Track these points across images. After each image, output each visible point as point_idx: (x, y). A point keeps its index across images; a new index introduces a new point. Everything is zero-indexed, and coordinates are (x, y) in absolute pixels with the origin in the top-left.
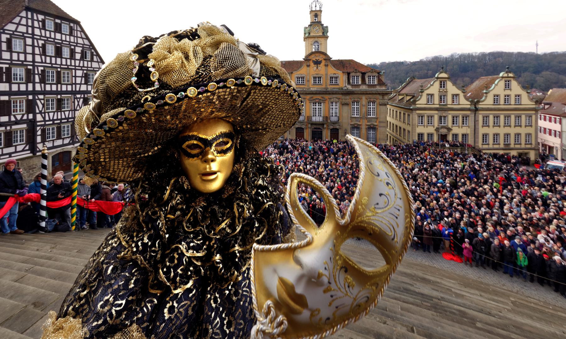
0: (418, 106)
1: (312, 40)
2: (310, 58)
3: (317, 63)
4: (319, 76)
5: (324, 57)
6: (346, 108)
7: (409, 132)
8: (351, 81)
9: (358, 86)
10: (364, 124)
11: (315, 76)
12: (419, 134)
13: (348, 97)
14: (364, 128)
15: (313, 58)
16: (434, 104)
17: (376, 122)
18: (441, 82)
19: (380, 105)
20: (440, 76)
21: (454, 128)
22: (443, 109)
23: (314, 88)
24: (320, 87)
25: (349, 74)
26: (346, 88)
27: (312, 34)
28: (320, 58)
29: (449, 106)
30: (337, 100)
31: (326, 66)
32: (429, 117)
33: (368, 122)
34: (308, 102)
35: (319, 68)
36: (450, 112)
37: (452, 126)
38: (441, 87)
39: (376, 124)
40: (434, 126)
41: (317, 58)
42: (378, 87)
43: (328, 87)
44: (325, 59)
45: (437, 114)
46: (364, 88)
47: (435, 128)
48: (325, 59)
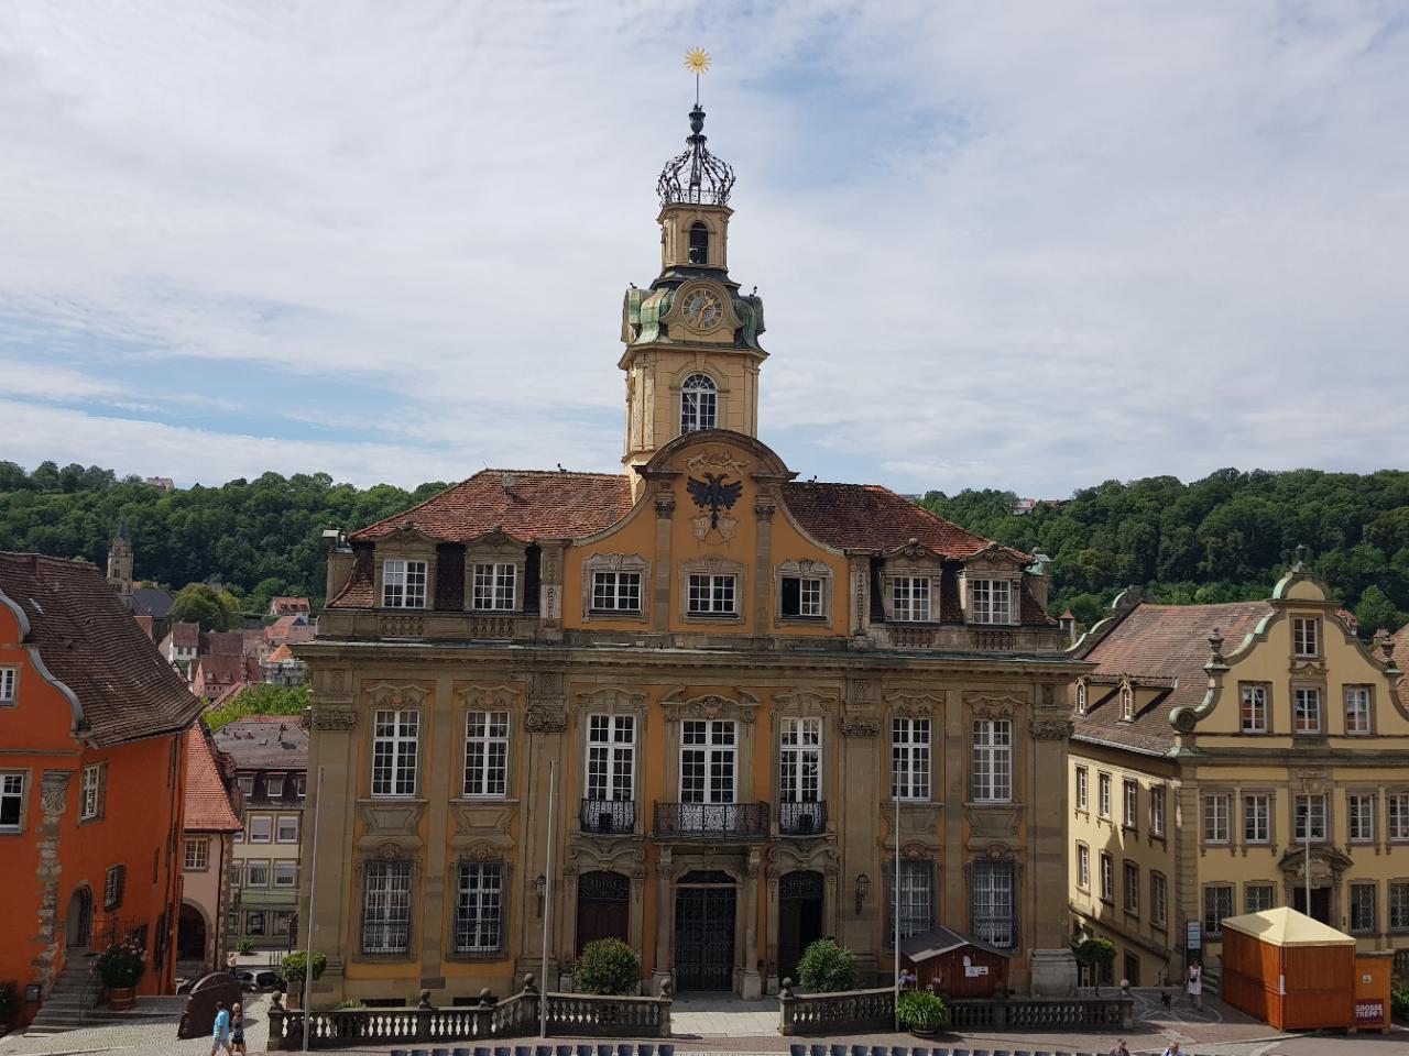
0: (1201, 742)
1: (676, 363)
2: (676, 465)
3: (715, 495)
7: (1157, 879)
8: (888, 603)
9: (923, 630)
10: (955, 843)
11: (699, 568)
12: (1209, 891)
13: (872, 692)
14: (953, 864)
15: (696, 465)
16: (1270, 734)
17: (1015, 831)
18: (1298, 624)
19: (1036, 737)
20: (1291, 595)
21: (1357, 855)
22: (1309, 753)
25: (877, 563)
26: (861, 642)
27: (677, 333)
28: (734, 469)
29: (1334, 744)
32: (1250, 800)
33: (976, 830)
35: (725, 525)
36: (1339, 774)
37: (1349, 846)
38: (1299, 649)
39: (1014, 842)
40: (1273, 848)
42: (1021, 640)
43: (772, 631)
45: (1285, 784)
47: (1280, 855)
48: (756, 480)
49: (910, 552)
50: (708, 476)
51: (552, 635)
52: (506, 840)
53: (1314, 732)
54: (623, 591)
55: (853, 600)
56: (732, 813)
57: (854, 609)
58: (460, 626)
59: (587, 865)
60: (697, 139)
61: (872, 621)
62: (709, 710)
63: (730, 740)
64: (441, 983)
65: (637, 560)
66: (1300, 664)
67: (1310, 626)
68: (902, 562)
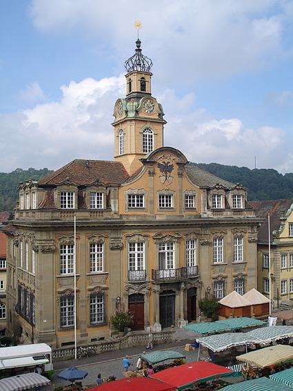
3: (166, 169)
4: (170, 192)
5: (177, 160)
6: (205, 249)
9: (221, 211)
15: (160, 160)
23: (161, 217)
24: (171, 214)
26: (205, 216)
28: (171, 160)
30: (195, 235)
31: (180, 175)
33: (235, 271)
34: (152, 242)
39: (244, 273)
41: (166, 161)
43: (183, 214)
44: (178, 164)
46: (228, 214)
48: (178, 164)
49: (217, 187)
50: (164, 162)
51: (116, 216)
52: (105, 286)
54: (138, 201)
55: (202, 203)
56: (174, 271)
58: (87, 214)
59: (132, 292)
62: (167, 239)
63: (172, 248)
64: (87, 335)
65: (143, 190)
68: (215, 190)
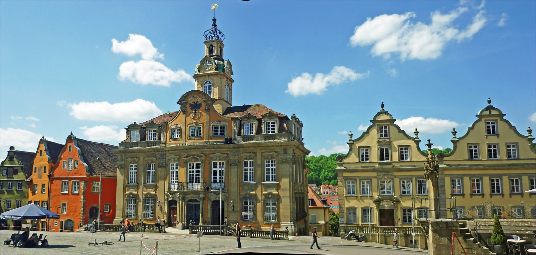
15: (191, 100)
28: (199, 100)
53: (387, 161)
57: (233, 134)
60: (215, 25)
61: (238, 135)
66: (381, 140)
67: (385, 128)
